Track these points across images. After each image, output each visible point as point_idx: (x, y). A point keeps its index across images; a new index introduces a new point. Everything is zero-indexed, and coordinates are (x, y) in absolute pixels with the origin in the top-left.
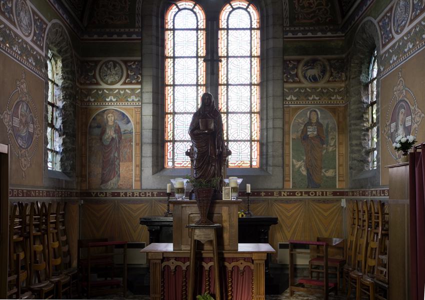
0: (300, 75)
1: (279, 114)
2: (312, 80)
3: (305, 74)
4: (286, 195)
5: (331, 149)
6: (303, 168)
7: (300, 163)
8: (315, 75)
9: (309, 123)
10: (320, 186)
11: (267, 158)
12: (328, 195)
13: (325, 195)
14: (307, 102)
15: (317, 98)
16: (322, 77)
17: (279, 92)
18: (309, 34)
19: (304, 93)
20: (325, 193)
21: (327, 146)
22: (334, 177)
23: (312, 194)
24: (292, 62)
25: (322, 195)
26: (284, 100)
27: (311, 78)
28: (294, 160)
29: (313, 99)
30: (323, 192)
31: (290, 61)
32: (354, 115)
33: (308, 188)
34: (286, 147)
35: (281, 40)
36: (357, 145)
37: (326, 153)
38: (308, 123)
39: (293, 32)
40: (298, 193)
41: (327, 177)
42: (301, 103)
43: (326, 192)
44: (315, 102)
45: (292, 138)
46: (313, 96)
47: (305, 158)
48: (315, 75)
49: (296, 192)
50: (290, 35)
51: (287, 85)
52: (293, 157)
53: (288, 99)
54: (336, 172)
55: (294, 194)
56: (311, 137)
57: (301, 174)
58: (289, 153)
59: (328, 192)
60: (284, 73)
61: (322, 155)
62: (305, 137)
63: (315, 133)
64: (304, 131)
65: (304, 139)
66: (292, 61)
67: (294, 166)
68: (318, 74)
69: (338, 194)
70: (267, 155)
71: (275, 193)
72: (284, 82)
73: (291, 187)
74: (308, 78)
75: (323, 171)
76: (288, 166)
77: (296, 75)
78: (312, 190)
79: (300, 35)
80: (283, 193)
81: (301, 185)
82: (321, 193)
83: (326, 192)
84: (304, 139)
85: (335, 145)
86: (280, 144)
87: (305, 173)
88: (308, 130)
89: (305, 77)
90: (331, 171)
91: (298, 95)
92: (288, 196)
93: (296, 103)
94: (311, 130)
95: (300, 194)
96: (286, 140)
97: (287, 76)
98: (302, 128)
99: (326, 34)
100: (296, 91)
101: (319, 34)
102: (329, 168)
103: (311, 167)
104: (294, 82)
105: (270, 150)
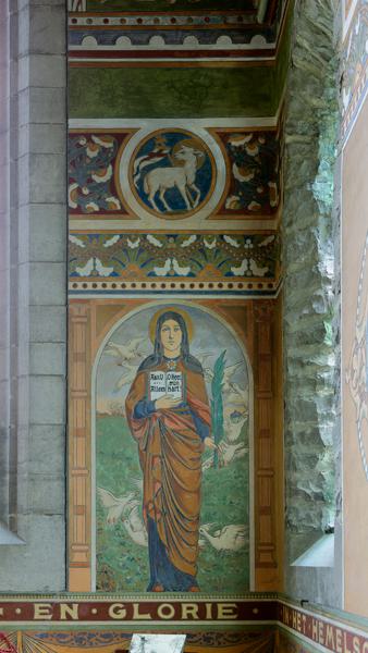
0: (124, 184)
1: (53, 326)
2: (166, 206)
3: (140, 183)
4: (74, 614)
7: (123, 500)
8: (175, 189)
9: (156, 360)
10: (194, 584)
11: (14, 484)
12: (220, 616)
13: (209, 615)
14: (149, 284)
15: (184, 271)
16: (199, 196)
17: (54, 250)
18: (157, 43)
19: (141, 250)
20: (209, 607)
21: (216, 443)
23: (166, 611)
24: (96, 139)
25: (202, 615)
26: (69, 275)
27: (161, 197)
28: (103, 492)
29: (168, 275)
30: (202, 606)
31: (90, 140)
33: (151, 589)
34: (76, 444)
35: (61, 59)
37: (213, 466)
38: (152, 358)
39: (103, 34)
40: (116, 610)
41: (218, 553)
42: (129, 287)
43: (215, 605)
44: (178, 284)
45: (97, 413)
46: (168, 262)
47: (140, 484)
48: (175, 189)
49: (108, 605)
50: (90, 43)
51: (77, 224)
52: (101, 478)
53: (84, 271)
54: (247, 536)
55: (102, 611)
56: (161, 410)
57: (125, 541)
58: (88, 466)
59: (220, 606)
60: (70, 181)
61: (200, 474)
62: (140, 412)
63: (178, 394)
64: (140, 388)
65: (137, 416)
66: (97, 135)
67: (101, 511)
68: (187, 186)
69: (18, 611)
70: (14, 472)
71: (37, 606)
72: (71, 211)
73: (94, 589)
74: (151, 199)
75: (204, 528)
76: (83, 510)
77: (112, 187)
78: (166, 599)
79: (124, 44)
80: (64, 608)
81: (128, 582)
82: (196, 608)
83: (215, 605)
84: (137, 416)
86: (57, 434)
87: (140, 537)
88: (152, 383)
89: (142, 195)
91: (112, 257)
92: (81, 618)
93: (109, 288)
94: (161, 384)
95: (123, 613)
96: (76, 420)
97: (79, 190)
98: (132, 376)
99: (214, 42)
100: (109, 243)
101: (190, 43)
103: (164, 514)
104: (104, 212)
105: (22, 457)
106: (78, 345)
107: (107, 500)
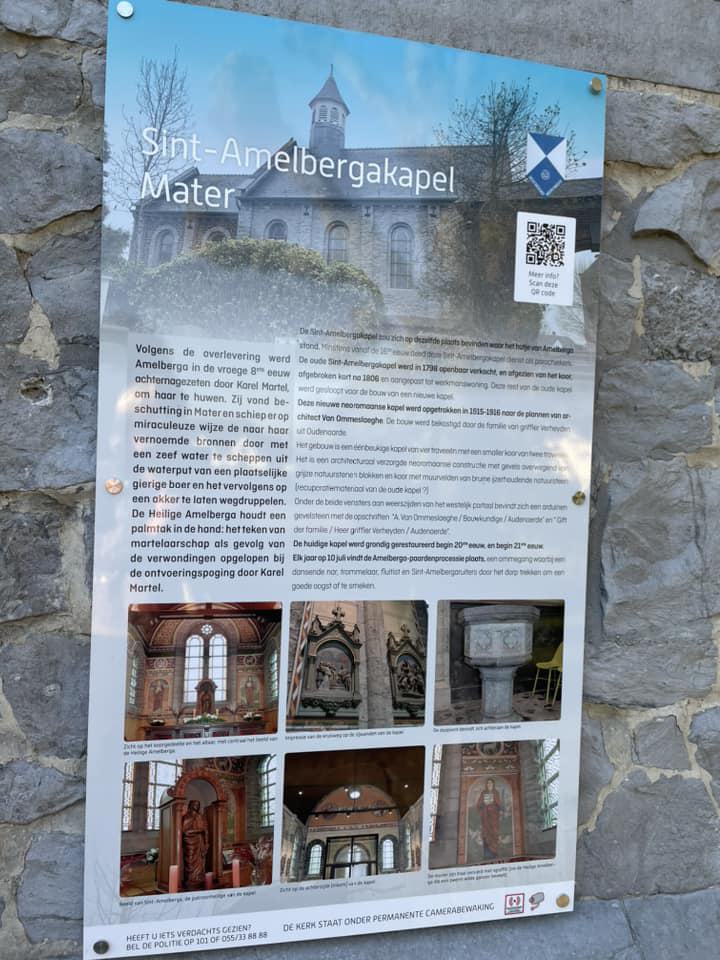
5: (506, 815)
6: (479, 838)
9: (486, 791)
22: (511, 844)
26: (462, 770)
32: (527, 776)
36: (532, 806)
51: (464, 757)
53: (466, 769)
63: (492, 800)
64: (482, 798)
67: (469, 836)
72: (463, 755)
76: (463, 837)
85: (510, 811)
87: (481, 843)
89: (482, 750)
90: (508, 837)
91: (475, 766)
102: (507, 834)
104: (472, 755)
106: (464, 788)
107: (471, 833)
